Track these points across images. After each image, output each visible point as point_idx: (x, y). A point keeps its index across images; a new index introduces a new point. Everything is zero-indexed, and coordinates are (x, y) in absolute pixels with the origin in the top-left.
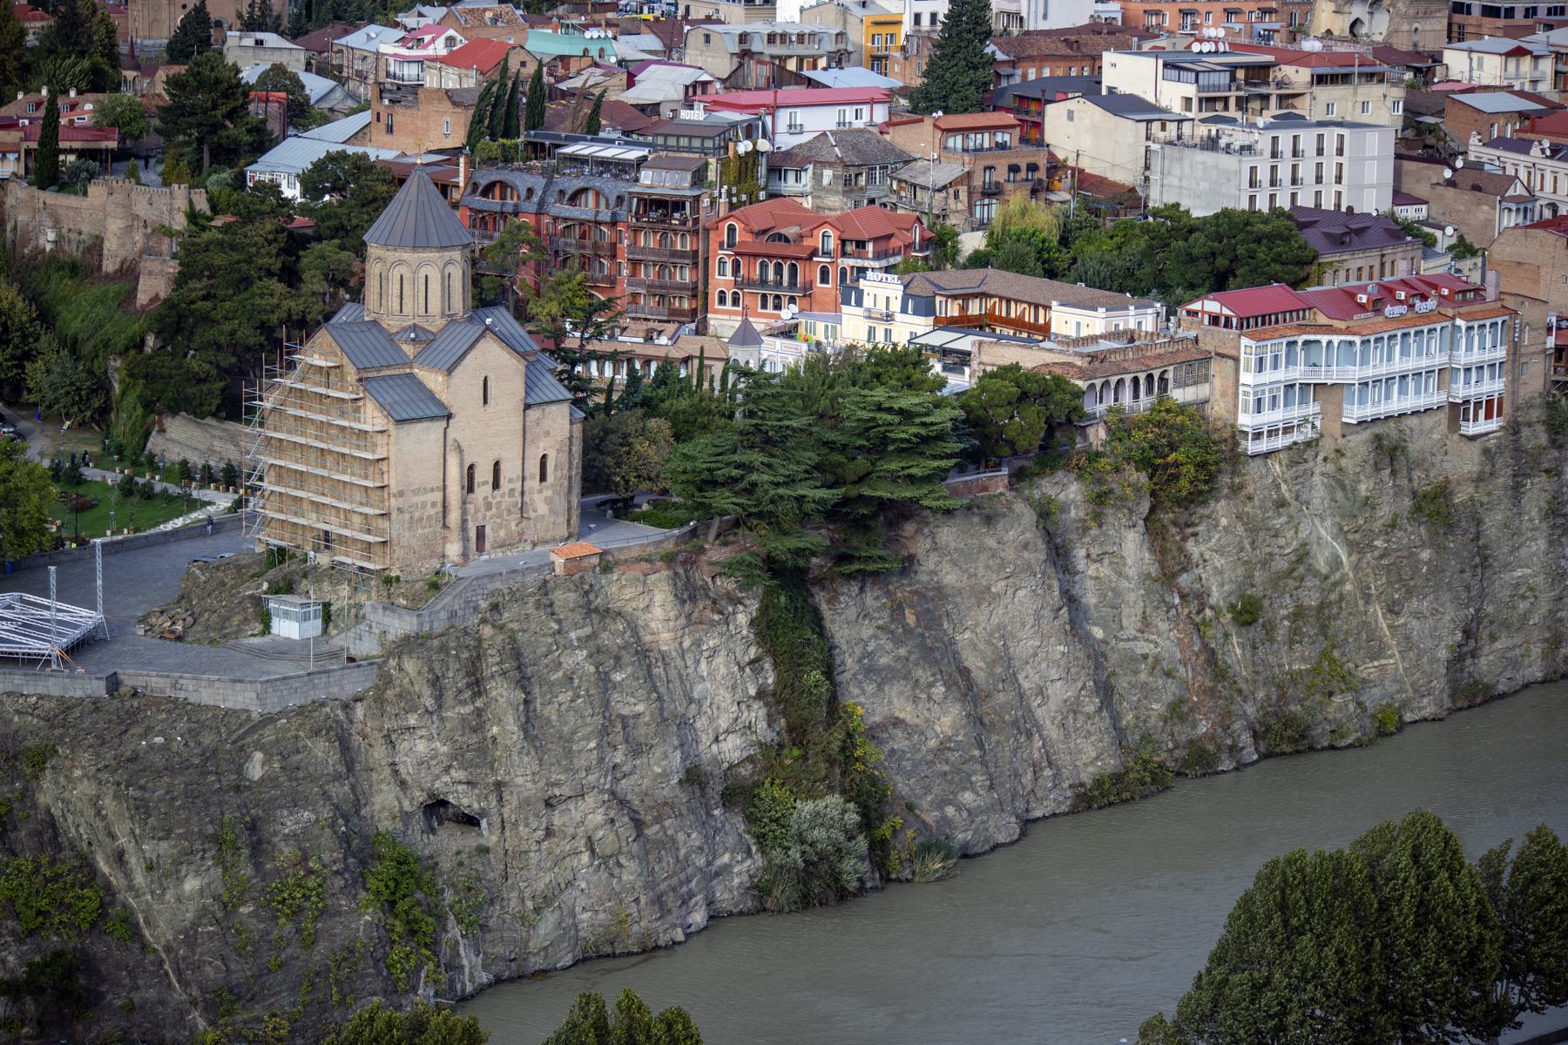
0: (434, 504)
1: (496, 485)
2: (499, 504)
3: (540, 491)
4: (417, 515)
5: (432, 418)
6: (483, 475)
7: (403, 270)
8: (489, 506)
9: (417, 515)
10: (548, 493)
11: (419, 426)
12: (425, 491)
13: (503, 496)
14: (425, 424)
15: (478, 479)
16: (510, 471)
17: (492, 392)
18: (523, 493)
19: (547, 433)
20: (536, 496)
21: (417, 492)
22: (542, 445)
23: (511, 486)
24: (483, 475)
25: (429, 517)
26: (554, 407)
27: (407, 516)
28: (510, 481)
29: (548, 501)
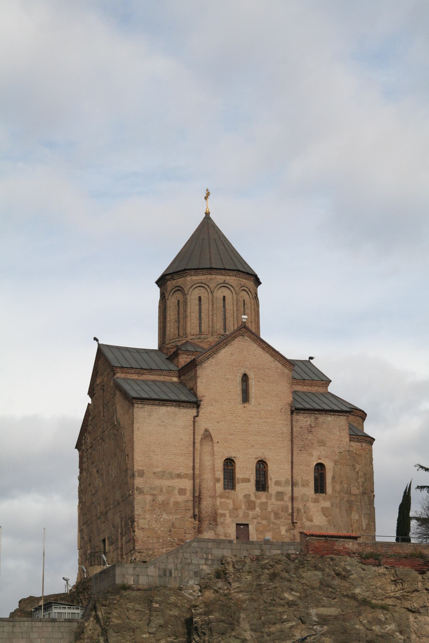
0: (182, 491)
1: (262, 484)
2: (264, 506)
3: (316, 501)
4: (160, 498)
5: (179, 403)
6: (245, 471)
7: (179, 295)
8: (251, 505)
9: (160, 498)
10: (327, 504)
11: (163, 410)
12: (171, 476)
13: (269, 497)
14: (171, 409)
15: (239, 475)
16: (277, 472)
17: (253, 390)
18: (292, 498)
19: (322, 443)
20: (311, 505)
21: (162, 475)
22: (316, 453)
23: (280, 489)
24: (245, 471)
25: (176, 503)
26: (330, 418)
27: (149, 498)
28: (278, 483)
29: (324, 511)
